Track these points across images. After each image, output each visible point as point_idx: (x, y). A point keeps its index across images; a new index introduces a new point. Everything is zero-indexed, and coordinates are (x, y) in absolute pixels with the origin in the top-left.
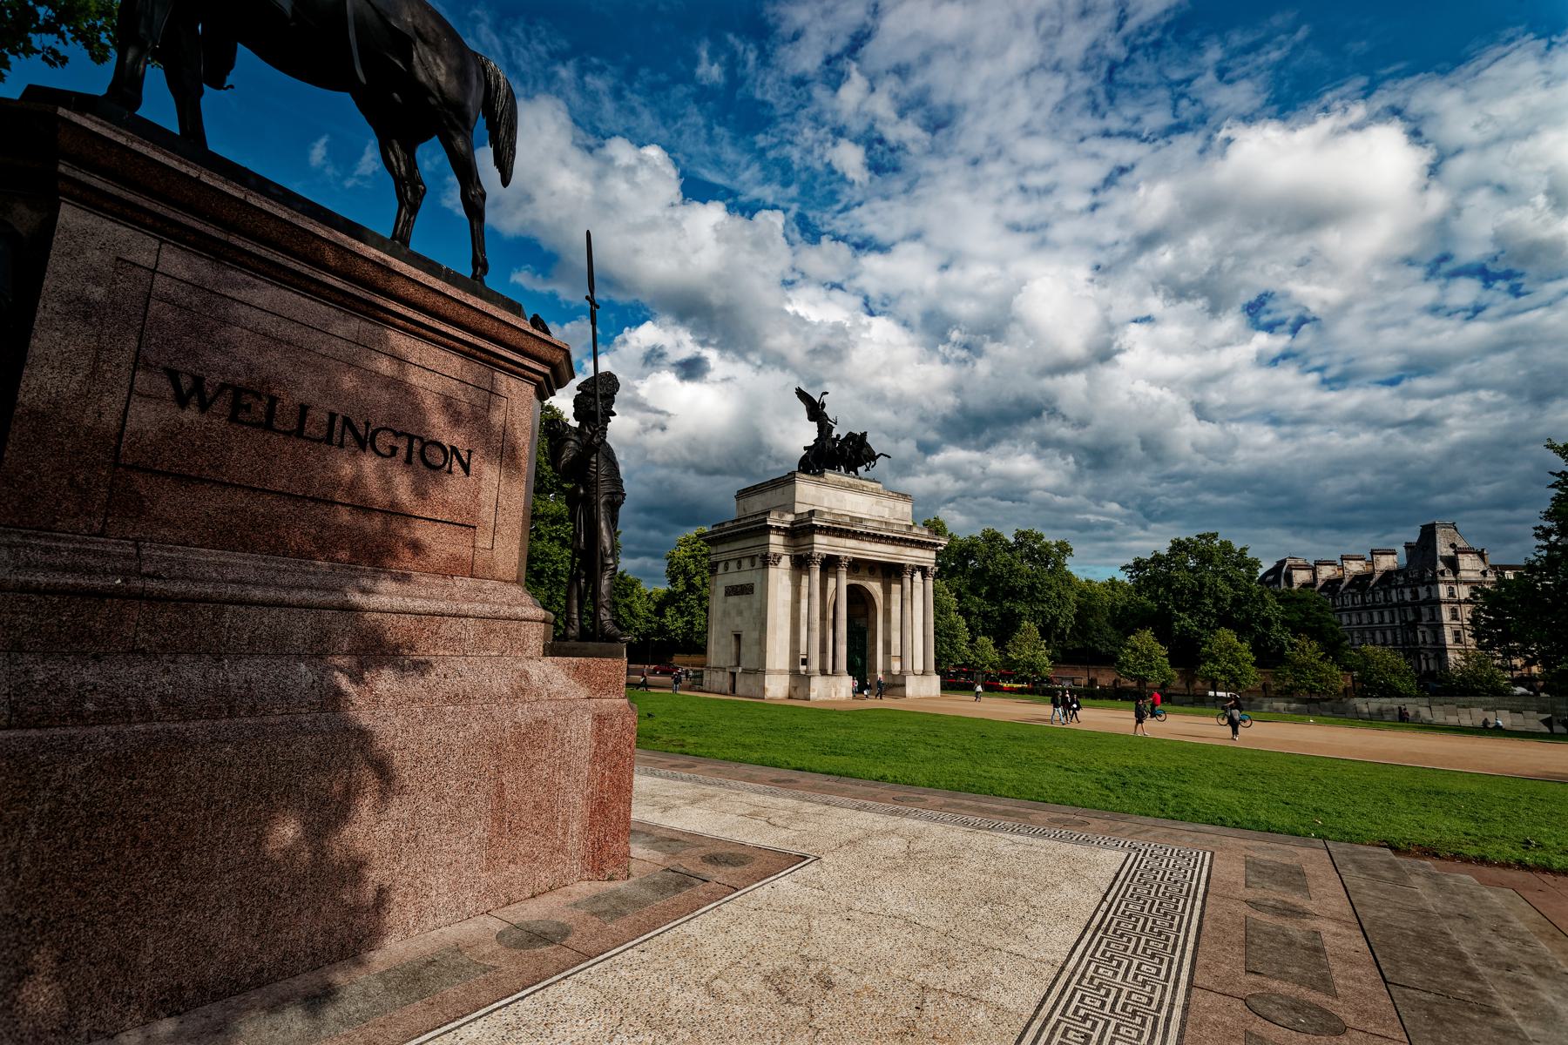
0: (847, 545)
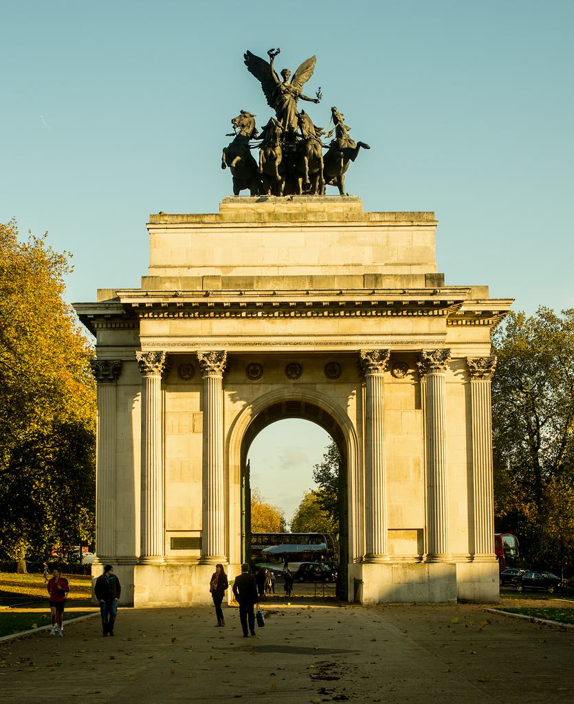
0: (215, 332)
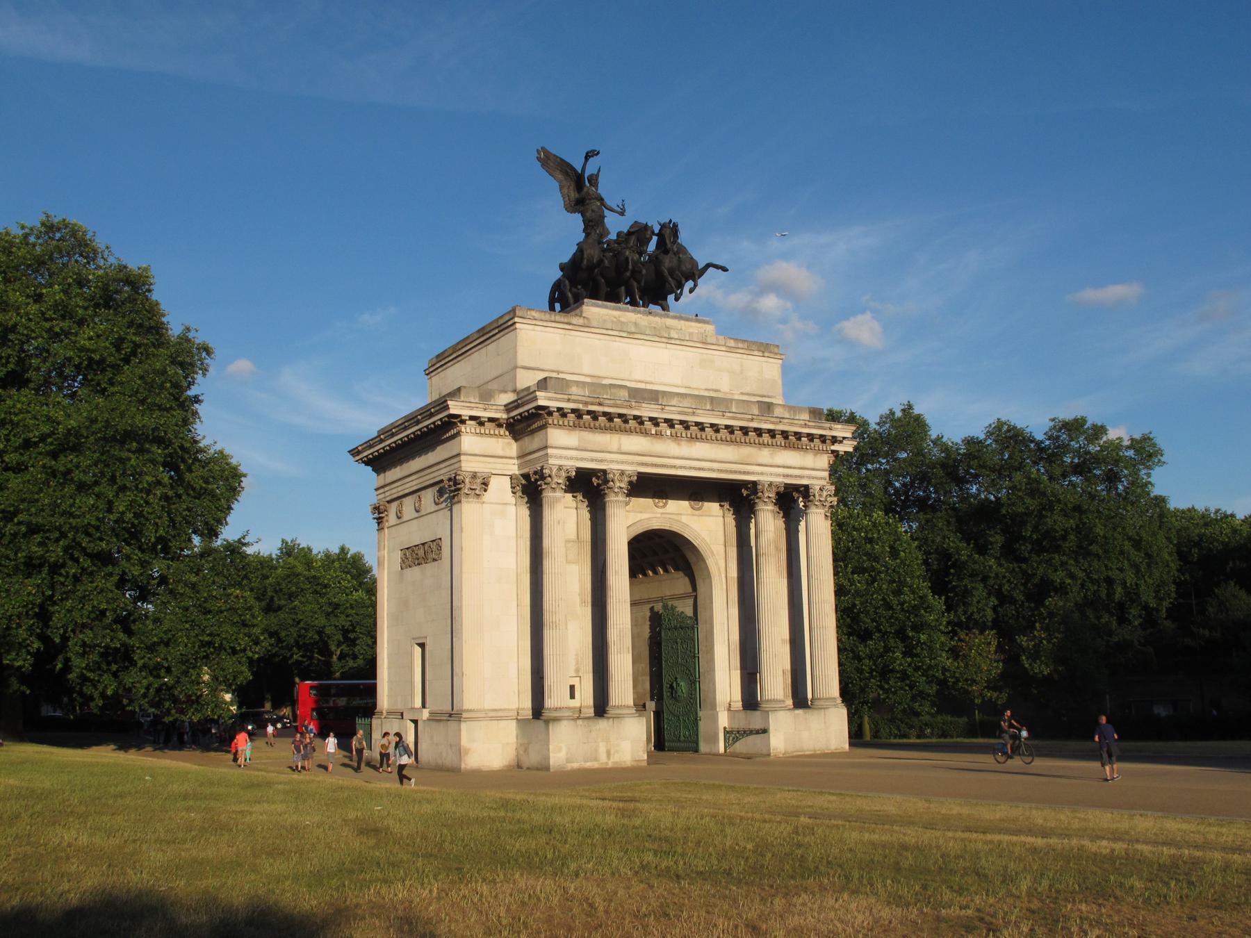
0: (625, 448)
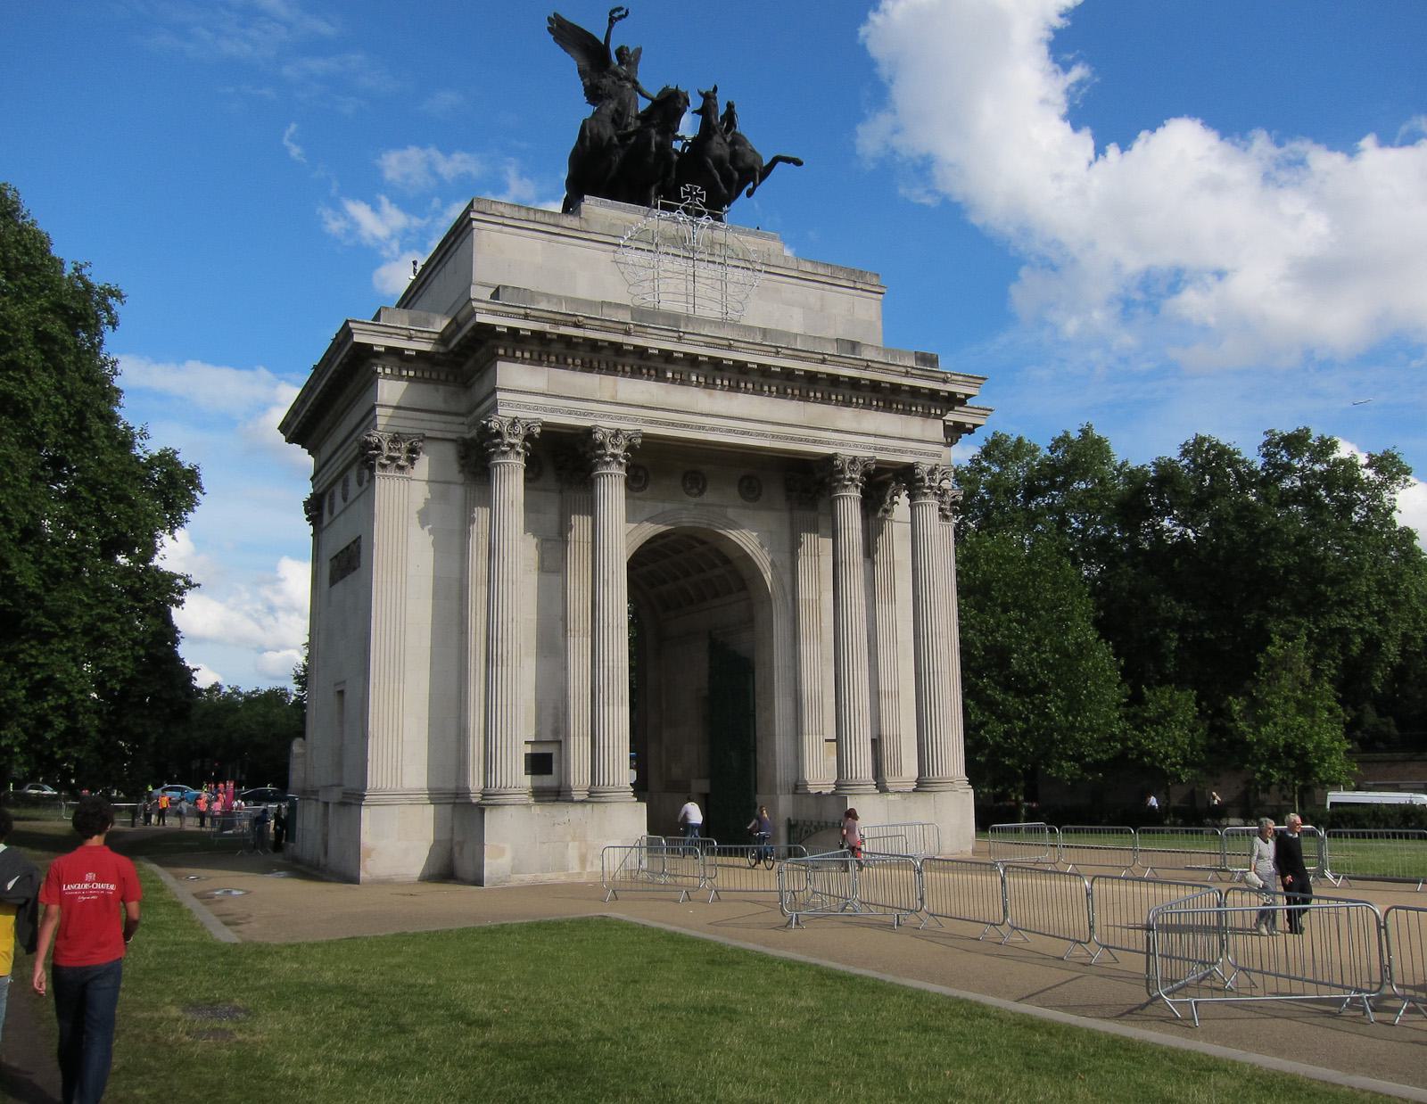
0: (621, 397)
